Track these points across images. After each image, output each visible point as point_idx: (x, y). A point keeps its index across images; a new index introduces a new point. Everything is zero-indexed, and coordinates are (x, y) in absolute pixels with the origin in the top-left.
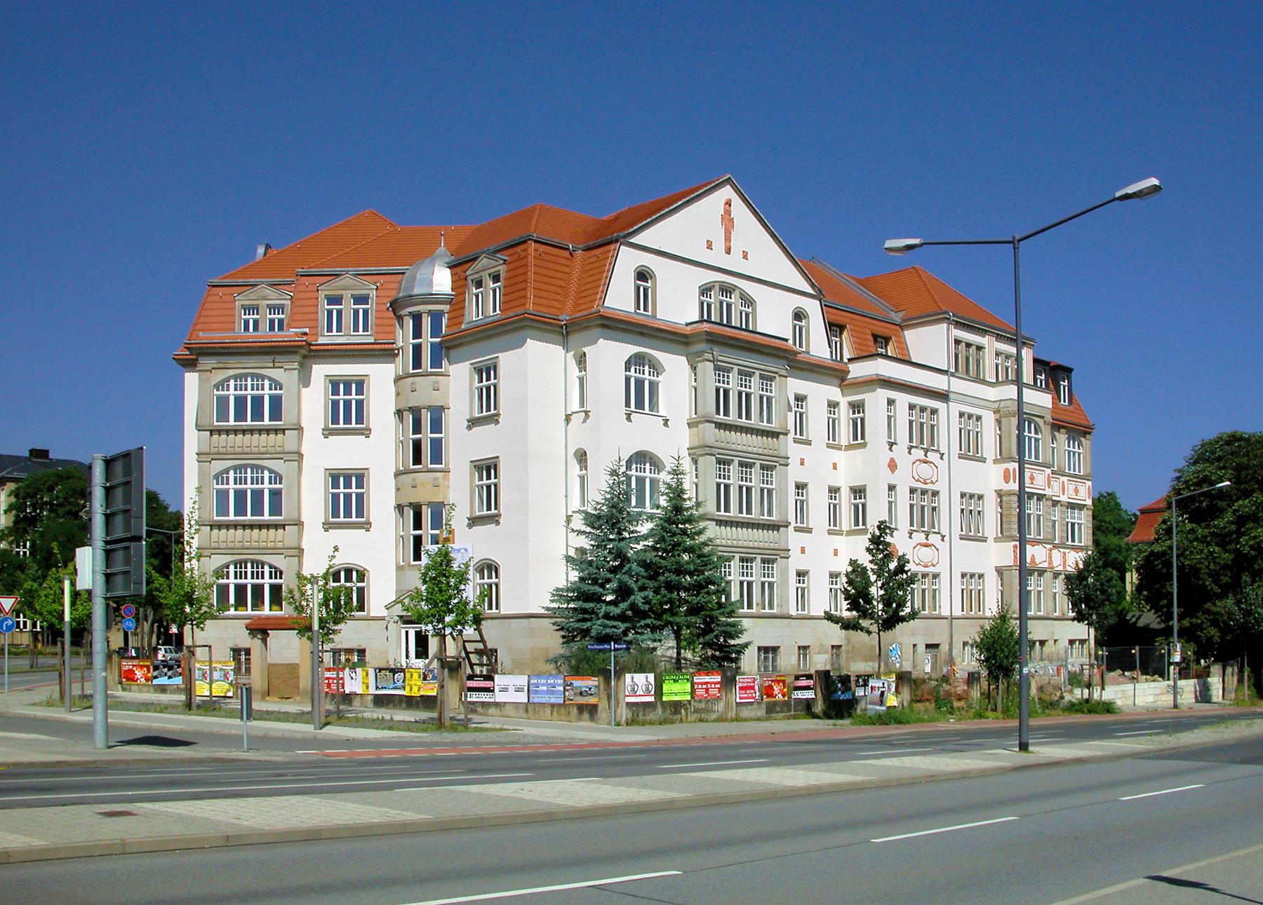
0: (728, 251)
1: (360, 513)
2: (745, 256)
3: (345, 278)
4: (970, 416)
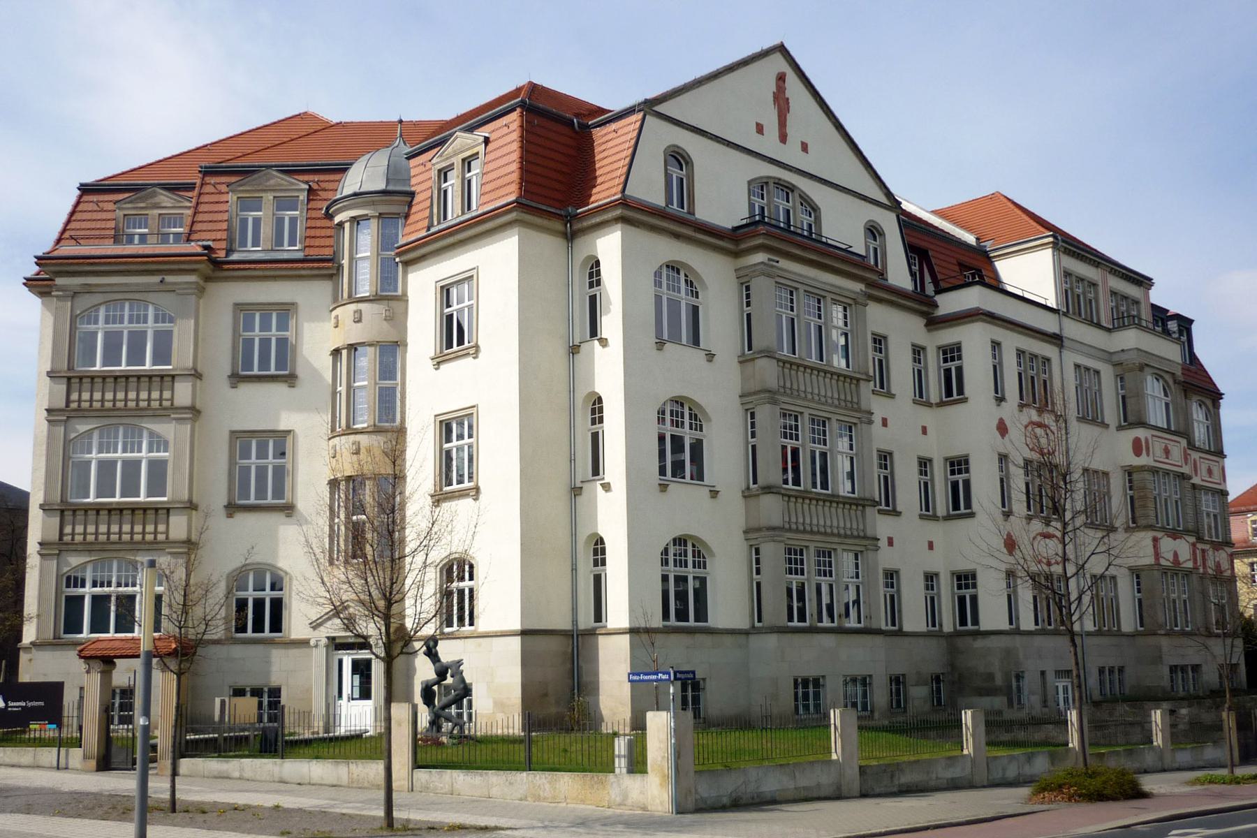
0: (783, 138)
2: (805, 147)
4: (1087, 369)
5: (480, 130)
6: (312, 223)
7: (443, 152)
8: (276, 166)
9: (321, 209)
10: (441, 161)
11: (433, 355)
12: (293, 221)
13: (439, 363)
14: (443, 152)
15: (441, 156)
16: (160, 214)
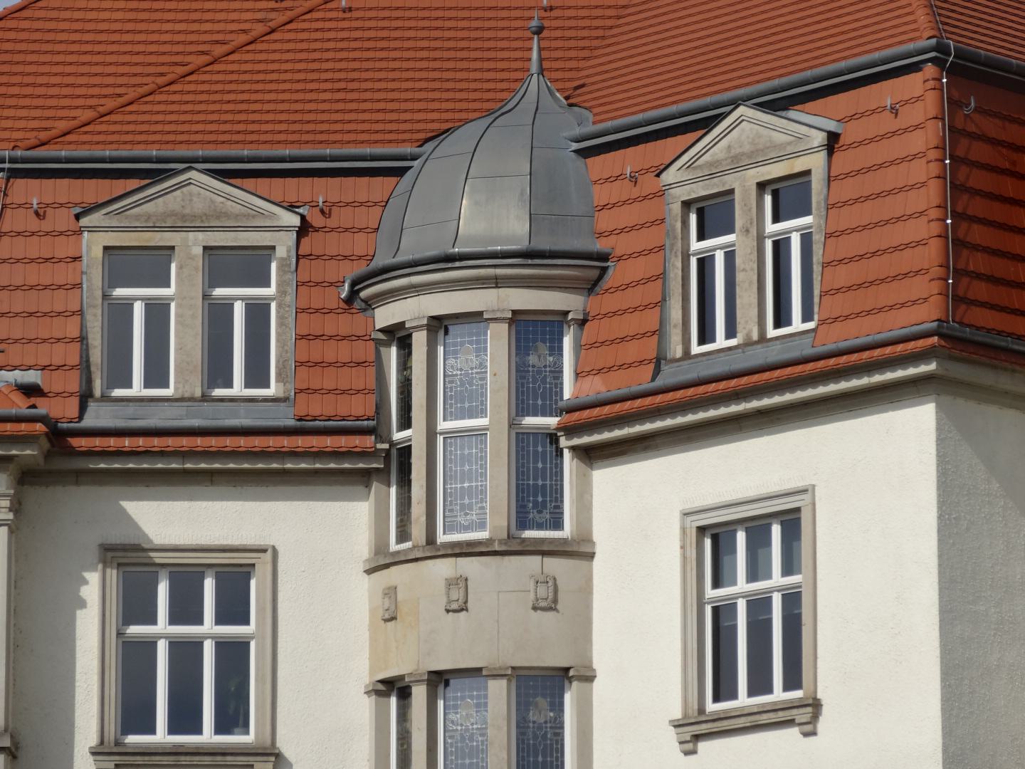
3: (180, 186)
5: (810, 106)
6: (315, 324)
7: (700, 155)
8: (206, 160)
9: (338, 284)
10: (694, 181)
11: (678, 715)
12: (258, 312)
13: (697, 738)
14: (700, 155)
15: (689, 166)
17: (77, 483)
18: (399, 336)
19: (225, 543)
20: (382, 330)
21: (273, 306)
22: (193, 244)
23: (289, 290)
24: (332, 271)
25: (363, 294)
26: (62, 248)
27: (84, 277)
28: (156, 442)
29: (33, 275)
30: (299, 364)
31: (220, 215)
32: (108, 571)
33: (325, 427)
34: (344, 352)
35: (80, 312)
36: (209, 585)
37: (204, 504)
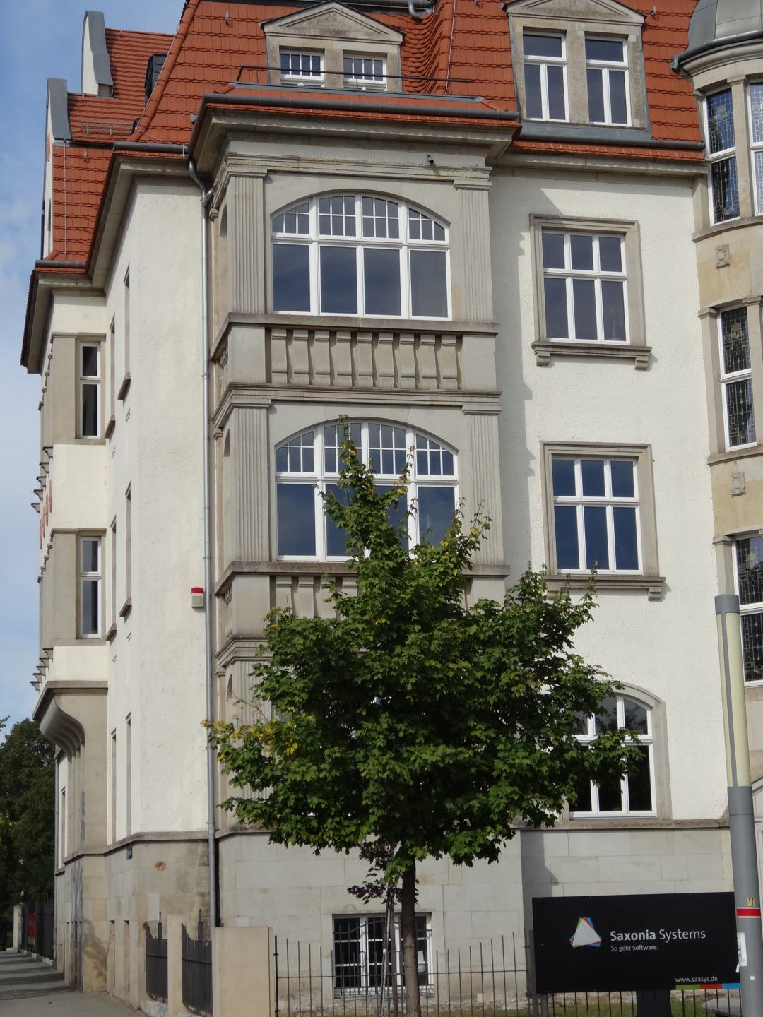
1: (627, 557)
6: (656, 83)
12: (617, 77)
16: (345, 52)
17: (513, 175)
18: (718, 93)
19: (606, 217)
20: (698, 90)
21: (627, 74)
22: (578, 30)
23: (639, 62)
24: (664, 53)
25: (686, 67)
26: (495, 26)
27: (512, 44)
28: (570, 147)
29: (479, 41)
30: (651, 107)
31: (594, 13)
32: (537, 232)
33: (675, 145)
34: (676, 101)
35: (510, 66)
36: (596, 245)
37: (593, 193)
